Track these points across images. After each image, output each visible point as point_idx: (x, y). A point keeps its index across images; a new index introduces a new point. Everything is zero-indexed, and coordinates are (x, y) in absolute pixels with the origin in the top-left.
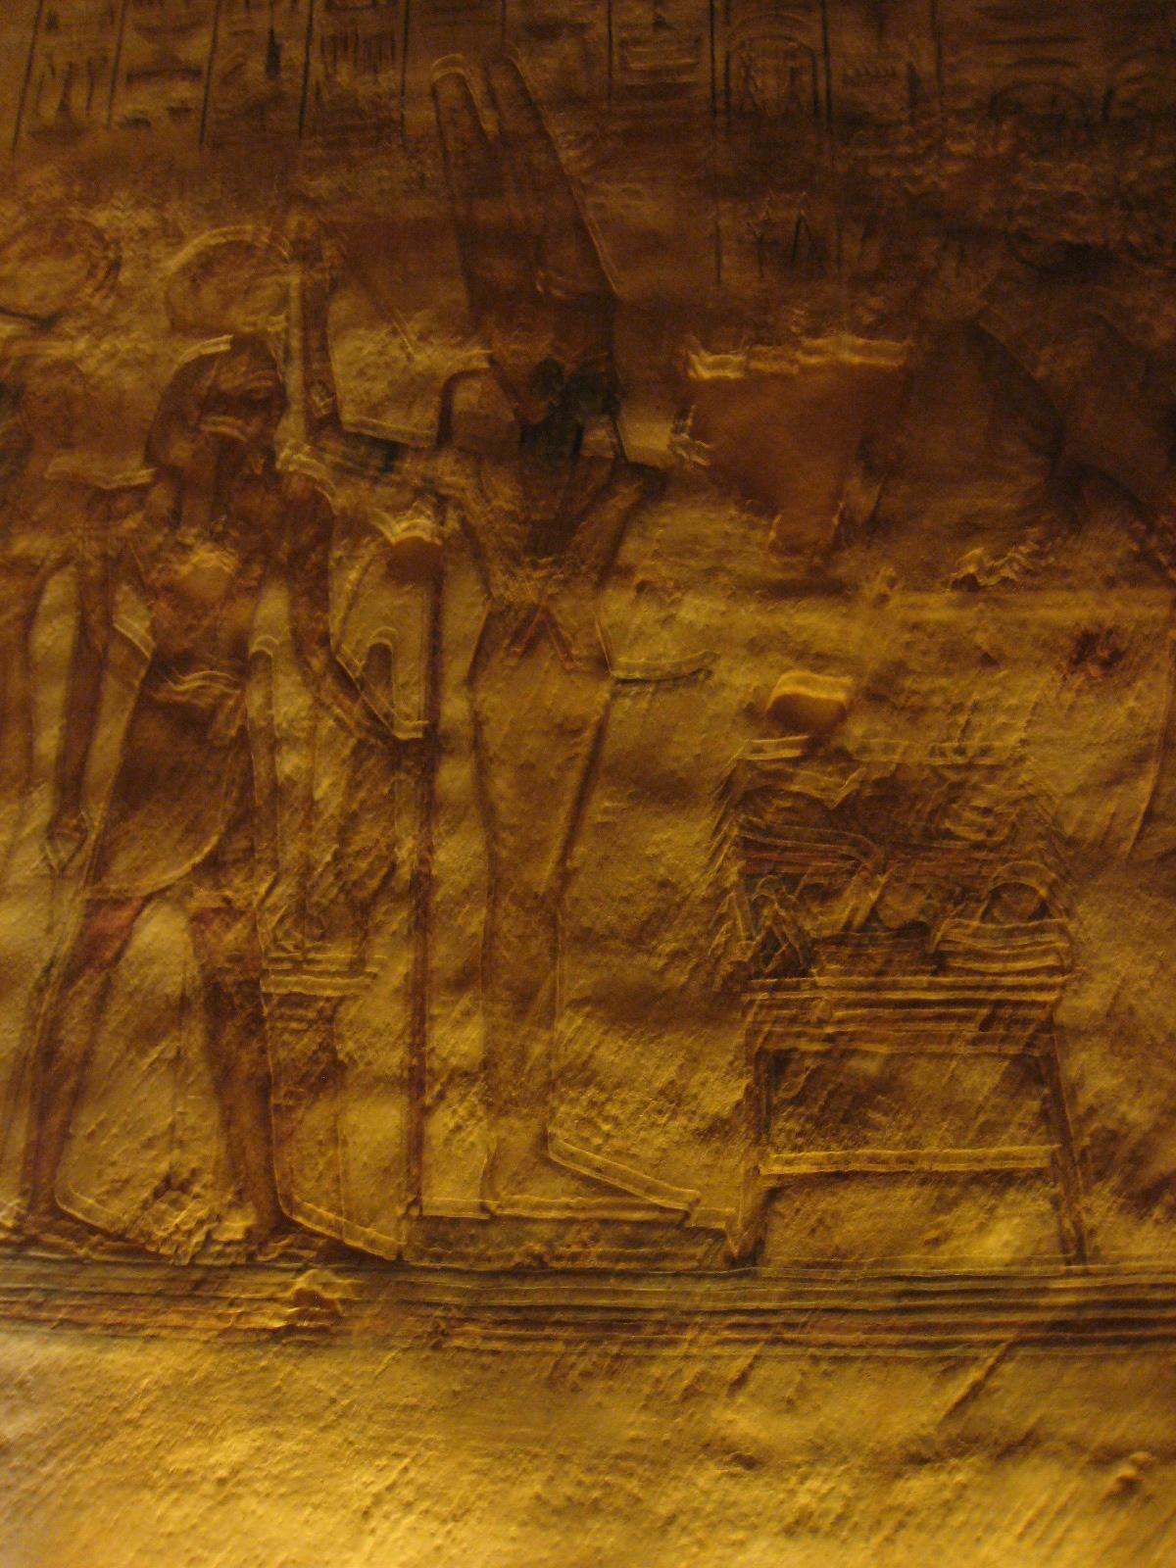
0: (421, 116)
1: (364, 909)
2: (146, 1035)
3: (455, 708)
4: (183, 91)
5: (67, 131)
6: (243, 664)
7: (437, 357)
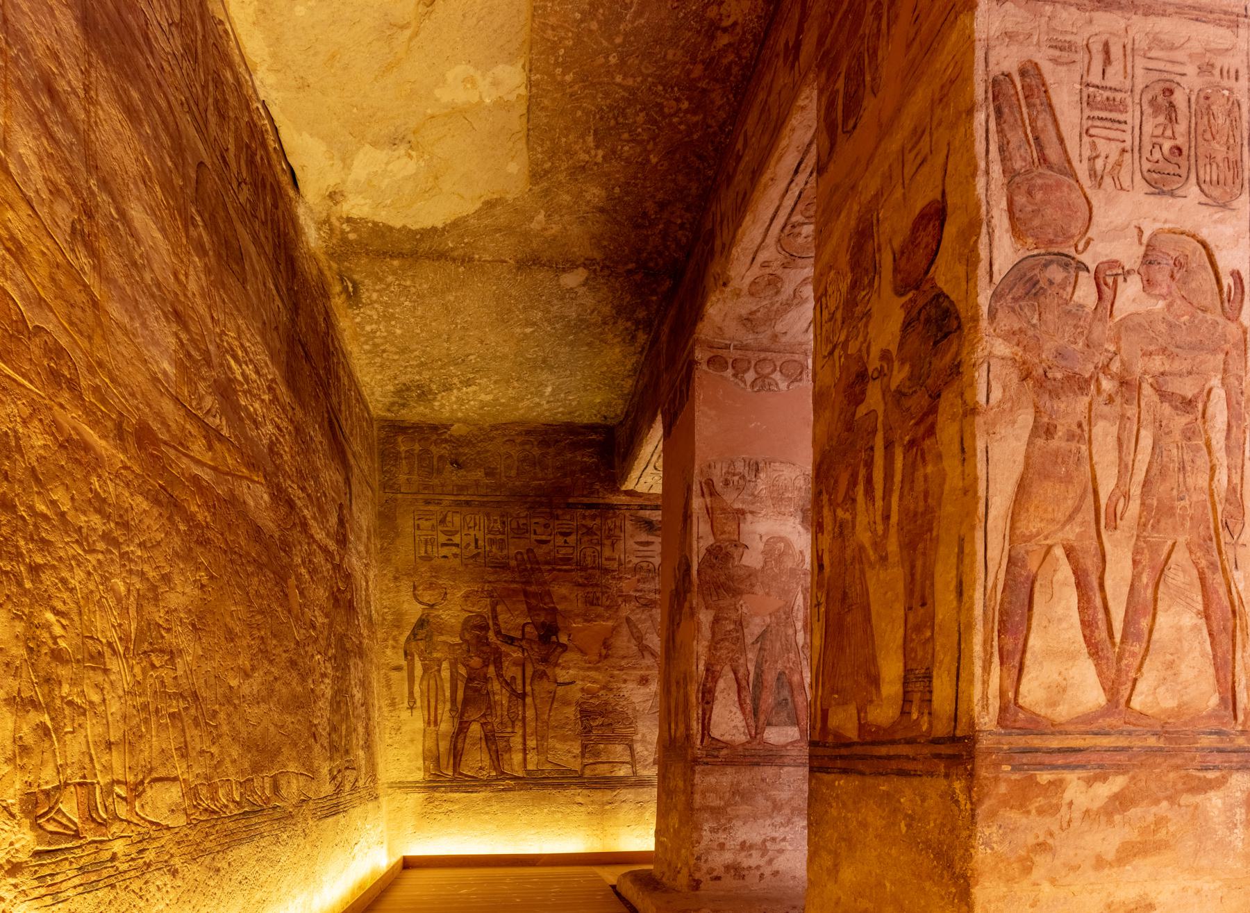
0: (513, 563)
1: (513, 722)
2: (474, 745)
3: (528, 688)
4: (455, 550)
5: (427, 558)
6: (486, 679)
7: (521, 621)
